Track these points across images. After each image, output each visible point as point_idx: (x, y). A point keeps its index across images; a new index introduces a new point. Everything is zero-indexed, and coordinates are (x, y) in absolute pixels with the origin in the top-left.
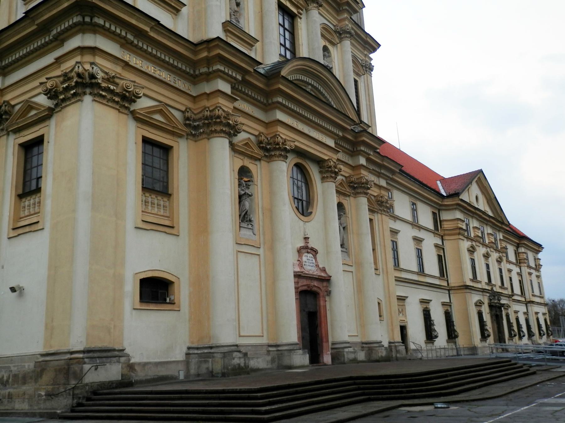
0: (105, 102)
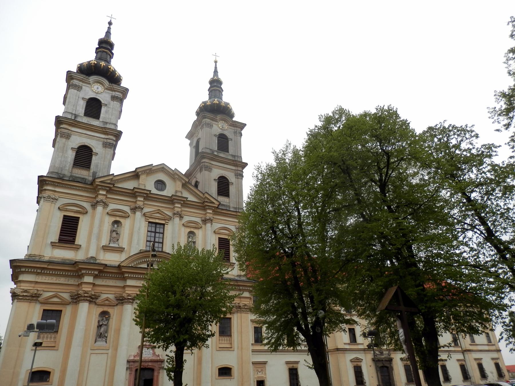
0: (22, 301)
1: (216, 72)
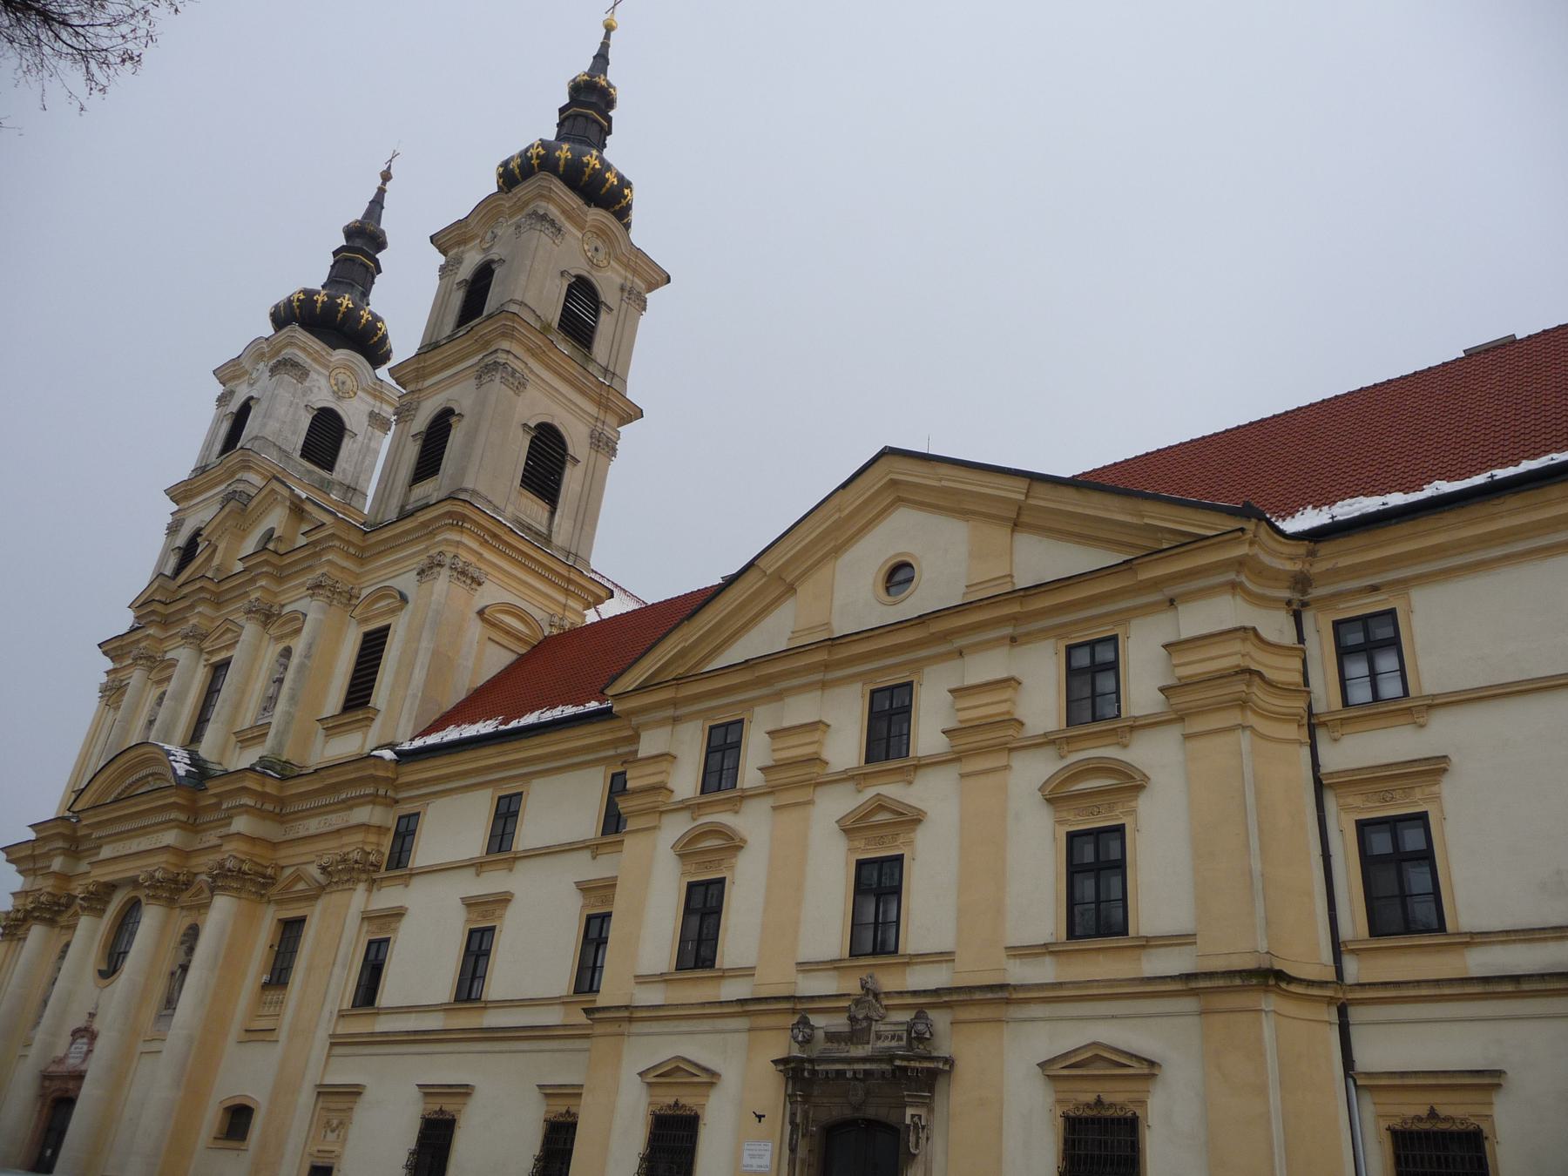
1: (601, 59)
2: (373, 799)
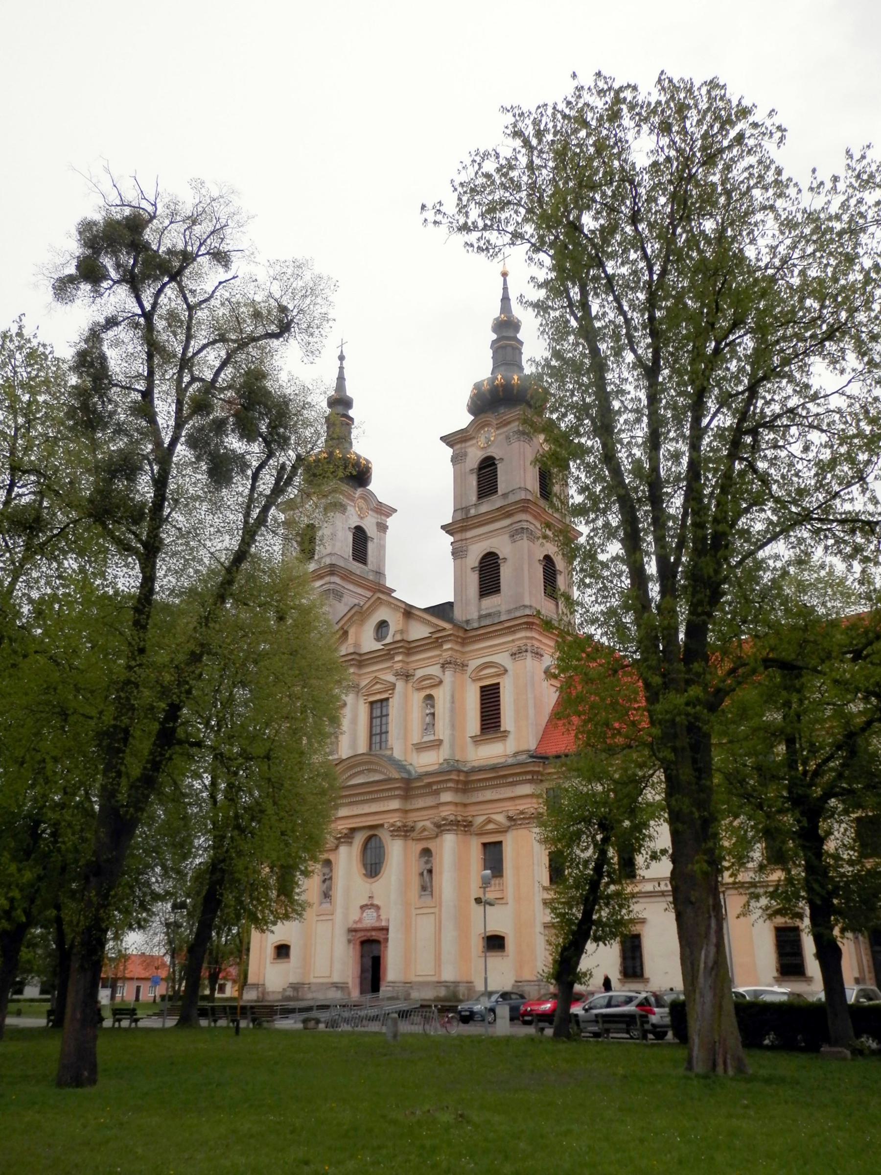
2: (530, 781)
